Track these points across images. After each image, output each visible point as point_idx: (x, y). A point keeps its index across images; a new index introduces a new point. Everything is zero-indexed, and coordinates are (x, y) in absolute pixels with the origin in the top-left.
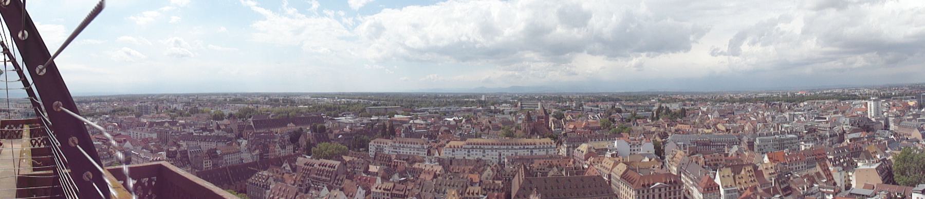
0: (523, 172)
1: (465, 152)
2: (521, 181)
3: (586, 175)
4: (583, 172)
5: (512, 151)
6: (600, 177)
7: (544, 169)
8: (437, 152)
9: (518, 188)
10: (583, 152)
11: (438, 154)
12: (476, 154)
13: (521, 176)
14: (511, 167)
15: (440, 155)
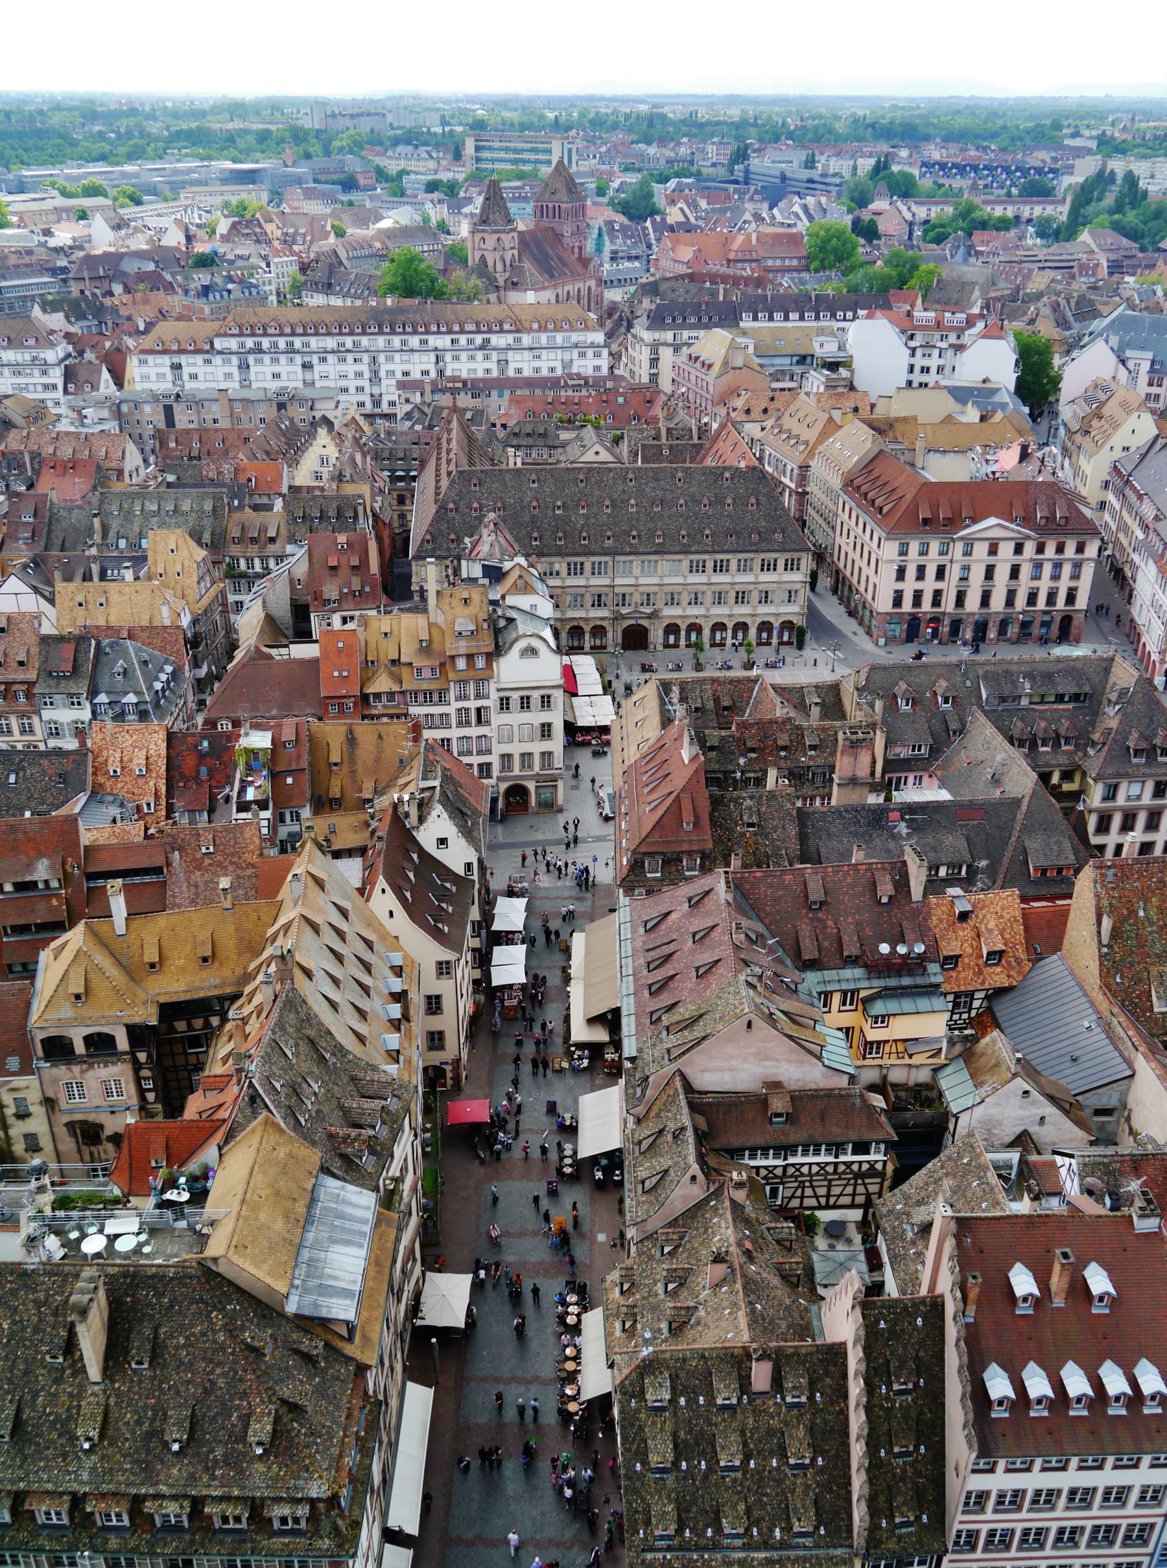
0: (454, 444)
1: (228, 370)
2: (445, 482)
3: (709, 462)
4: (698, 448)
5: (425, 358)
6: (756, 475)
7: (543, 435)
8: (105, 375)
9: (433, 509)
10: (710, 366)
11: (113, 387)
12: (276, 376)
13: (444, 461)
14: (418, 427)
15: (119, 382)
